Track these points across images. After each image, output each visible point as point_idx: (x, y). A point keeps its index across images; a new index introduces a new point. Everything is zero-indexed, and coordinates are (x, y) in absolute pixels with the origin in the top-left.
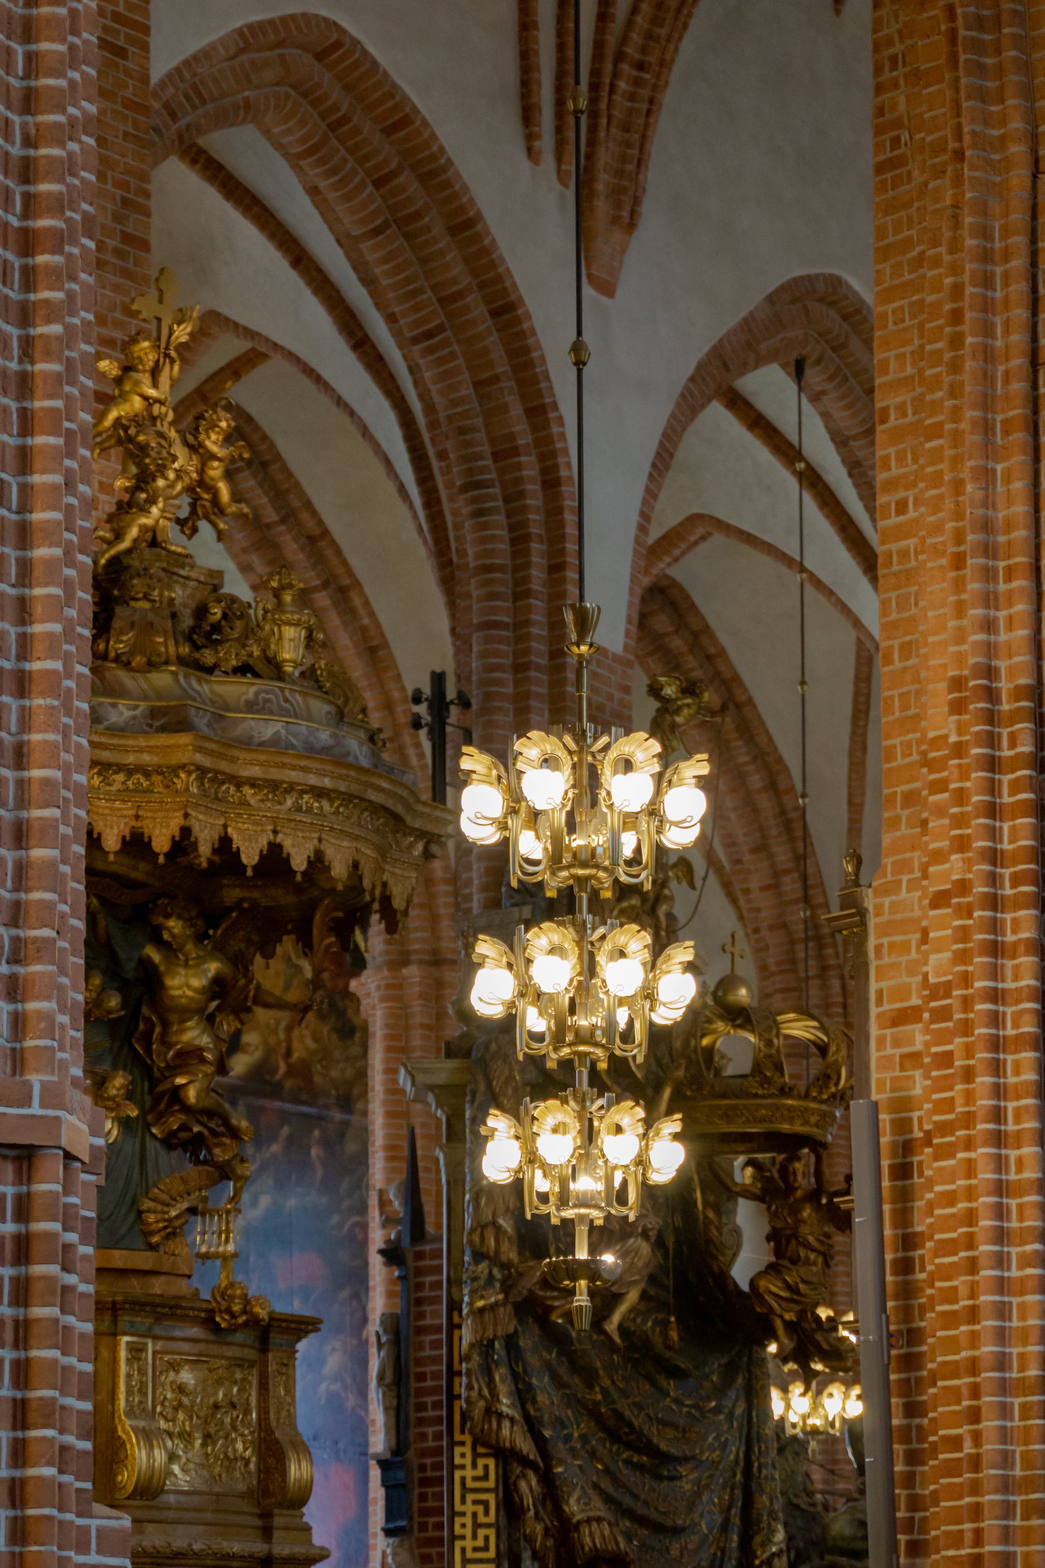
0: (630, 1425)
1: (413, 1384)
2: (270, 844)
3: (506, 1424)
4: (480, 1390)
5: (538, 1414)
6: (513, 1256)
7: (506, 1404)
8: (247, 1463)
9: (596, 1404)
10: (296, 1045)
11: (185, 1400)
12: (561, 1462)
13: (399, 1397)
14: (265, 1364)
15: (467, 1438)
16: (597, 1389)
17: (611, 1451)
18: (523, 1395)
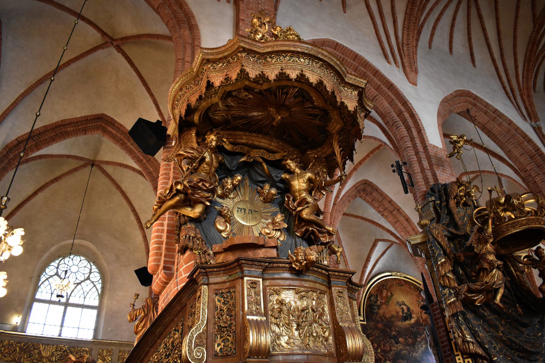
0: (516, 343)
1: (441, 345)
2: (280, 73)
3: (471, 344)
4: (458, 334)
5: (482, 340)
6: (456, 285)
7: (469, 338)
8: (327, 340)
9: (501, 337)
10: (423, 316)
11: (284, 308)
12: (495, 356)
13: (437, 350)
14: (331, 294)
15: (459, 353)
16: (500, 332)
17: (511, 353)
18: (474, 335)
